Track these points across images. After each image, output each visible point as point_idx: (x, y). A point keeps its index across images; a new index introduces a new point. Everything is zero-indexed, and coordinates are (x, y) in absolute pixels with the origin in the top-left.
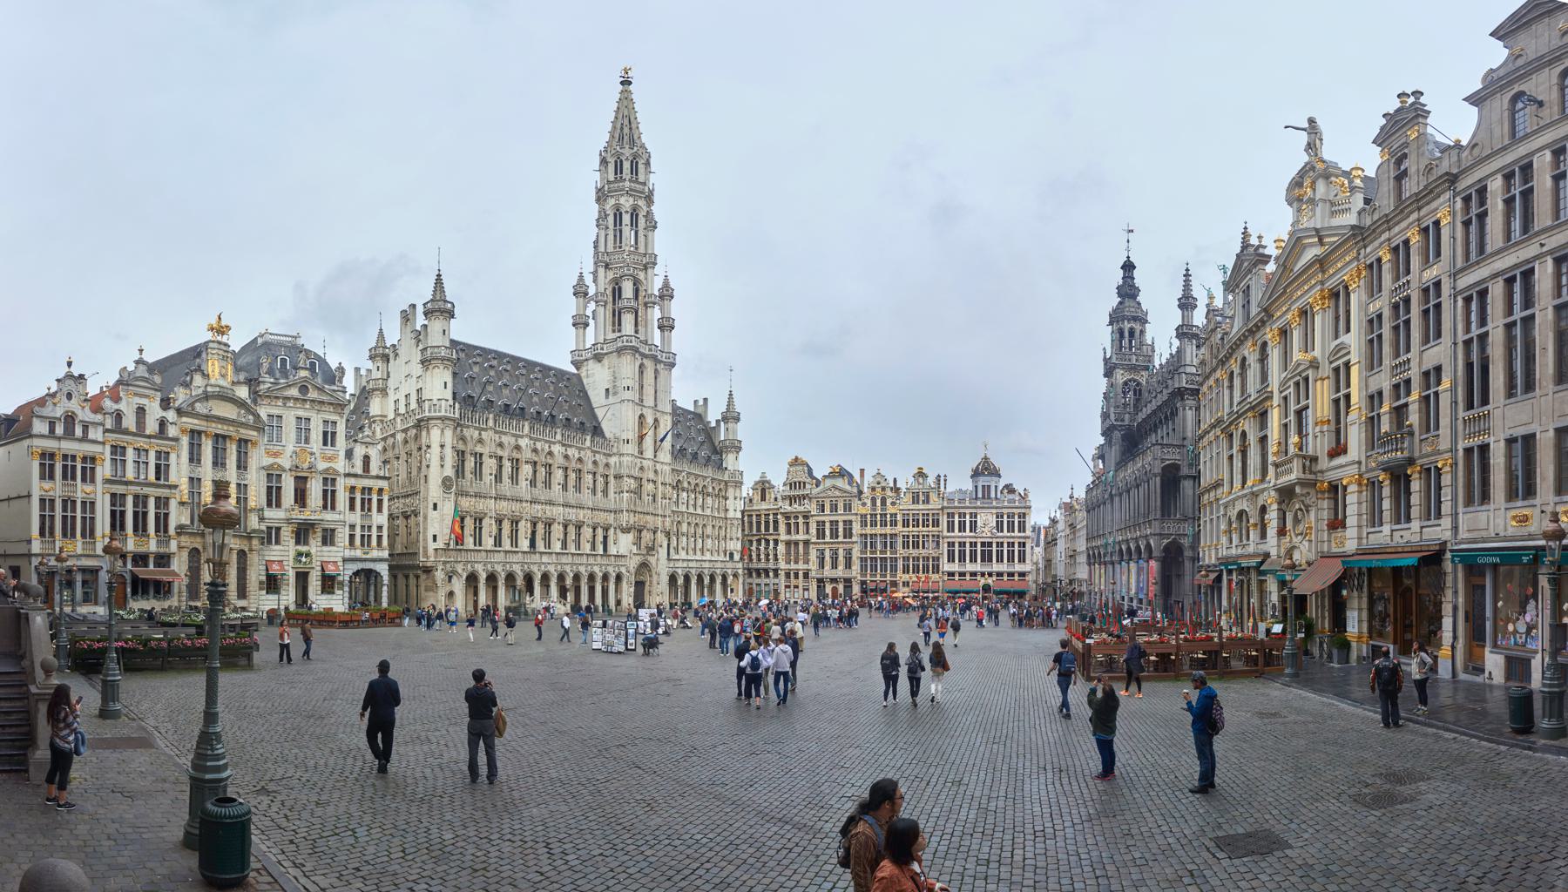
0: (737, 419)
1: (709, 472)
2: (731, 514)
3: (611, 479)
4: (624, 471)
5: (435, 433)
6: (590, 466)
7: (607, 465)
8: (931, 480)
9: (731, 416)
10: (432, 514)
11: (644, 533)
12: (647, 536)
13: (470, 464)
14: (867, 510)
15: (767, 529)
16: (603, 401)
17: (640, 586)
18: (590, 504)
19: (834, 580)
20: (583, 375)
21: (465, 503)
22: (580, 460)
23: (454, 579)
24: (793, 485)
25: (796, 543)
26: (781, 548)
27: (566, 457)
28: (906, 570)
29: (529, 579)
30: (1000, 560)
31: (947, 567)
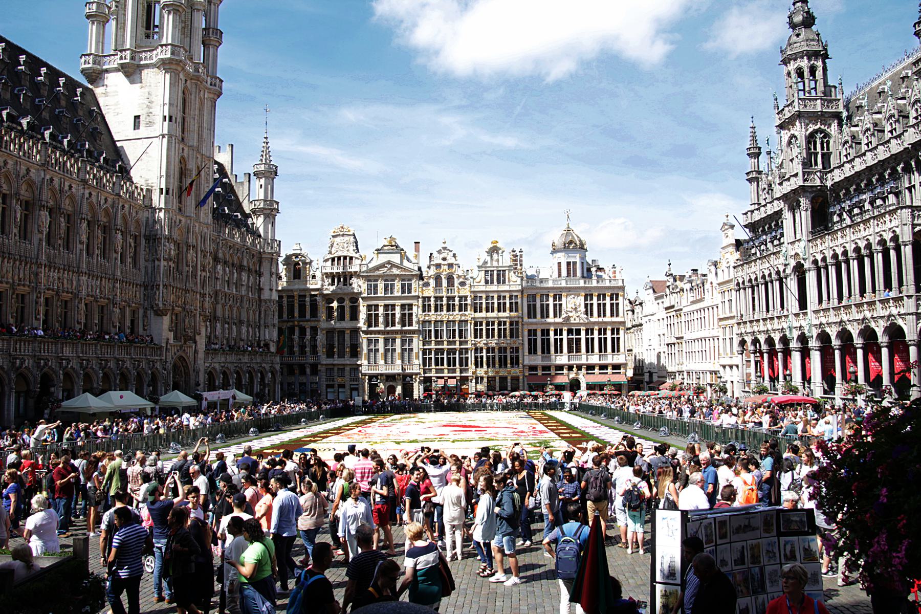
2: (266, 295)
14: (430, 292)
15: (302, 313)
19: (390, 378)
20: (98, 91)
25: (342, 332)
26: (321, 338)
30: (590, 349)
31: (528, 360)
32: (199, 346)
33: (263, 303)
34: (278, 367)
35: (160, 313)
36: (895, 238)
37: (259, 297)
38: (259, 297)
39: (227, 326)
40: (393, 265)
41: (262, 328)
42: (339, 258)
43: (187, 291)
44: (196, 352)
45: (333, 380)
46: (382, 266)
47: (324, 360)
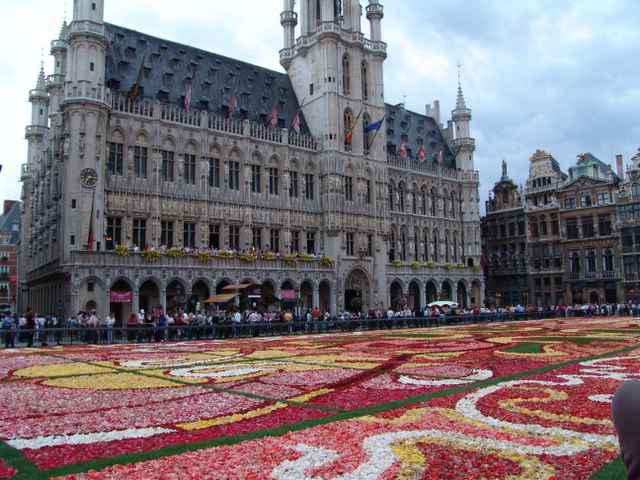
1: (440, 174)
2: (467, 218)
3: (316, 179)
4: (328, 169)
6: (287, 165)
7: (311, 164)
9: (462, 116)
12: (361, 241)
15: (512, 233)
16: (309, 98)
17: (351, 295)
18: (289, 206)
22: (275, 157)
23: (97, 288)
24: (536, 182)
26: (529, 251)
27: (257, 154)
32: (378, 262)
33: (466, 226)
34: (482, 279)
35: (334, 233)
37: (461, 218)
38: (461, 218)
39: (422, 244)
40: (584, 179)
41: (465, 246)
42: (539, 179)
43: (359, 215)
44: (375, 265)
45: (540, 289)
46: (579, 181)
47: (531, 271)
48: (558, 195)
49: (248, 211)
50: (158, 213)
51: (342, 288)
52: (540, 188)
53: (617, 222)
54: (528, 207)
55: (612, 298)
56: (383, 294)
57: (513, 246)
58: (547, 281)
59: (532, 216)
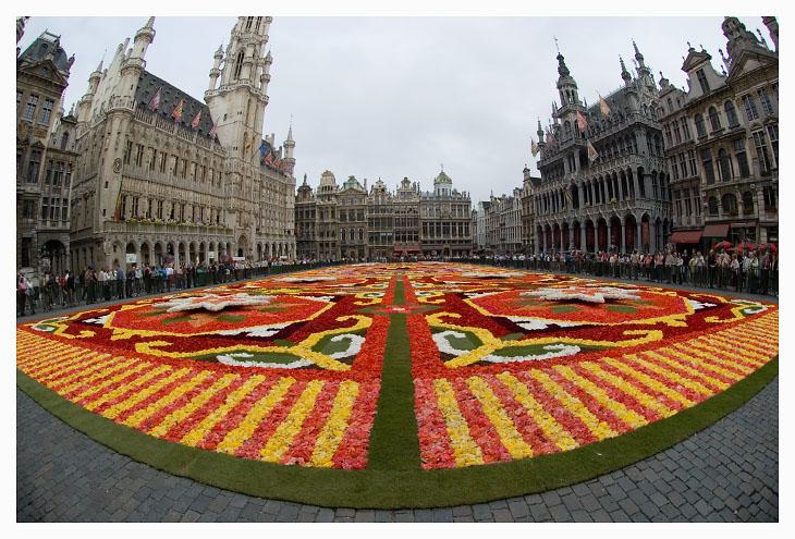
0: (294, 146)
1: (277, 177)
2: (288, 206)
3: (223, 174)
4: (233, 169)
5: (116, 122)
8: (411, 185)
9: (289, 145)
10: (104, 191)
11: (243, 214)
12: (245, 216)
13: (135, 151)
21: (128, 184)
24: (324, 188)
26: (317, 227)
28: (398, 239)
29: (171, 247)
35: (231, 212)
36: (629, 170)
40: (352, 189)
47: (318, 239)
48: (336, 196)
49: (191, 194)
50: (147, 194)
51: (237, 248)
52: (327, 191)
53: (367, 215)
54: (319, 202)
55: (361, 254)
56: (254, 253)
57: (308, 224)
58: (327, 245)
59: (320, 207)
